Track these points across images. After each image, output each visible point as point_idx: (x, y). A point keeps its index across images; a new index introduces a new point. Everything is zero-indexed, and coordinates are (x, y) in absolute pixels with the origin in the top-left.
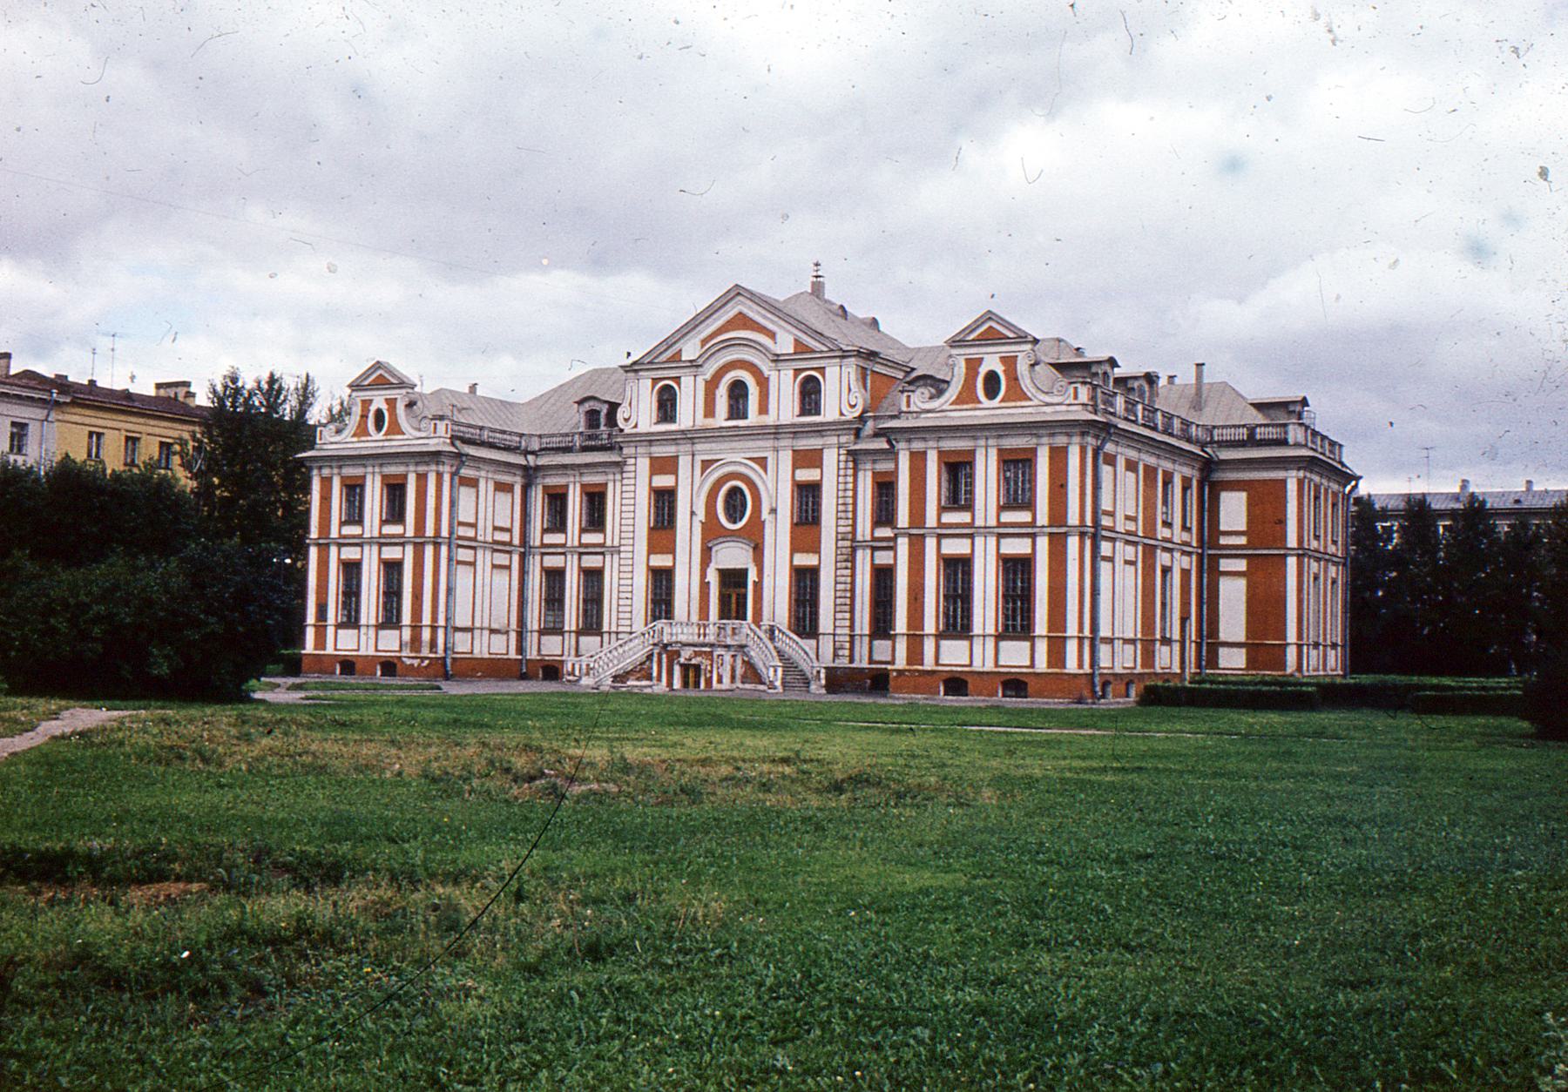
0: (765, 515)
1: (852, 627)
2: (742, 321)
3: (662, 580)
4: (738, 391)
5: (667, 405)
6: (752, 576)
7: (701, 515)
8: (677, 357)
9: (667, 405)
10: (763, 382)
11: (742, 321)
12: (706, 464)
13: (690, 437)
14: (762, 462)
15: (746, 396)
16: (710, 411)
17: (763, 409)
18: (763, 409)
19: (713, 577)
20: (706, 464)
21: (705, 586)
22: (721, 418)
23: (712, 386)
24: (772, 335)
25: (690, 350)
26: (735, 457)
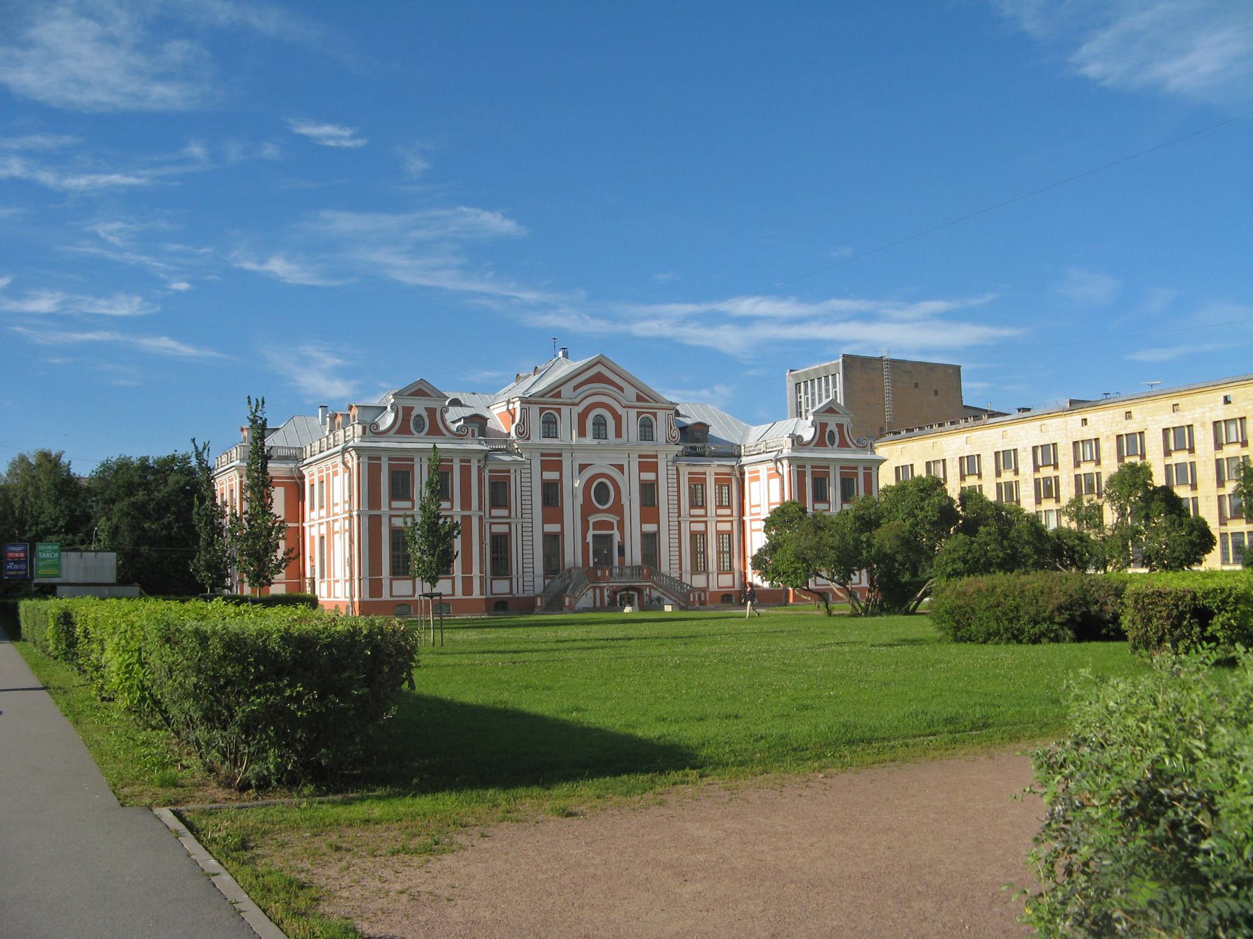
0: (625, 501)
1: (681, 569)
2: (599, 378)
3: (553, 543)
4: (600, 423)
5: (550, 426)
6: (617, 538)
7: (579, 501)
8: (558, 395)
9: (550, 426)
10: (618, 419)
11: (599, 378)
12: (582, 467)
13: (572, 449)
14: (620, 468)
15: (605, 424)
16: (582, 433)
17: (618, 434)
18: (618, 434)
19: (590, 539)
20: (582, 467)
21: (585, 545)
22: (589, 440)
23: (582, 417)
24: (622, 389)
25: (566, 391)
26: (602, 464)
